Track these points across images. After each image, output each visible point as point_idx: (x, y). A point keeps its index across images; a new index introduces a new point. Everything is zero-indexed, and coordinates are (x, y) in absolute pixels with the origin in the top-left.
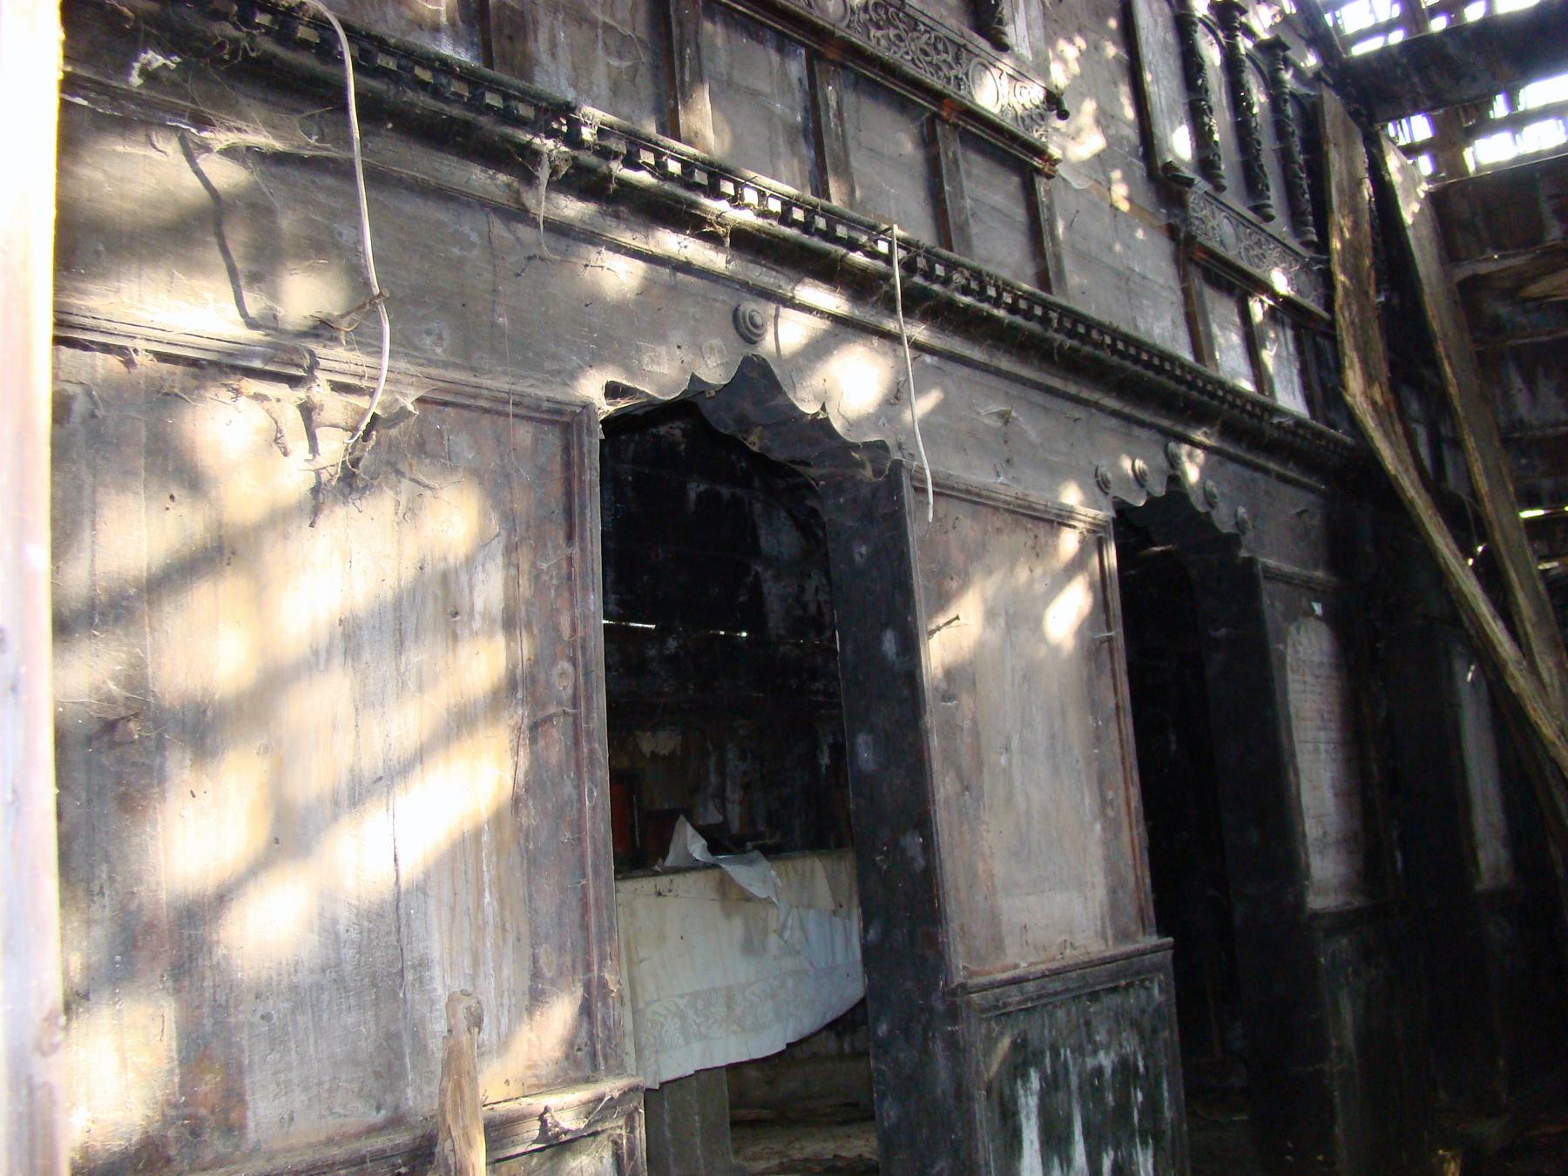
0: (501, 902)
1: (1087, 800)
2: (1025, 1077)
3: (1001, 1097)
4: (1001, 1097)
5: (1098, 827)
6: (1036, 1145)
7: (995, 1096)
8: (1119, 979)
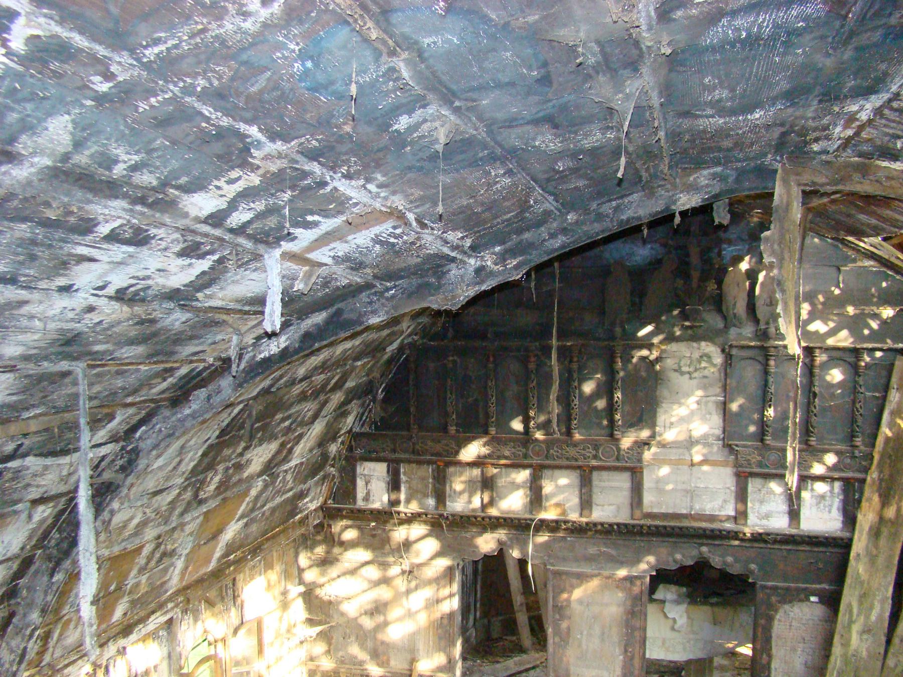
5: (621, 657)
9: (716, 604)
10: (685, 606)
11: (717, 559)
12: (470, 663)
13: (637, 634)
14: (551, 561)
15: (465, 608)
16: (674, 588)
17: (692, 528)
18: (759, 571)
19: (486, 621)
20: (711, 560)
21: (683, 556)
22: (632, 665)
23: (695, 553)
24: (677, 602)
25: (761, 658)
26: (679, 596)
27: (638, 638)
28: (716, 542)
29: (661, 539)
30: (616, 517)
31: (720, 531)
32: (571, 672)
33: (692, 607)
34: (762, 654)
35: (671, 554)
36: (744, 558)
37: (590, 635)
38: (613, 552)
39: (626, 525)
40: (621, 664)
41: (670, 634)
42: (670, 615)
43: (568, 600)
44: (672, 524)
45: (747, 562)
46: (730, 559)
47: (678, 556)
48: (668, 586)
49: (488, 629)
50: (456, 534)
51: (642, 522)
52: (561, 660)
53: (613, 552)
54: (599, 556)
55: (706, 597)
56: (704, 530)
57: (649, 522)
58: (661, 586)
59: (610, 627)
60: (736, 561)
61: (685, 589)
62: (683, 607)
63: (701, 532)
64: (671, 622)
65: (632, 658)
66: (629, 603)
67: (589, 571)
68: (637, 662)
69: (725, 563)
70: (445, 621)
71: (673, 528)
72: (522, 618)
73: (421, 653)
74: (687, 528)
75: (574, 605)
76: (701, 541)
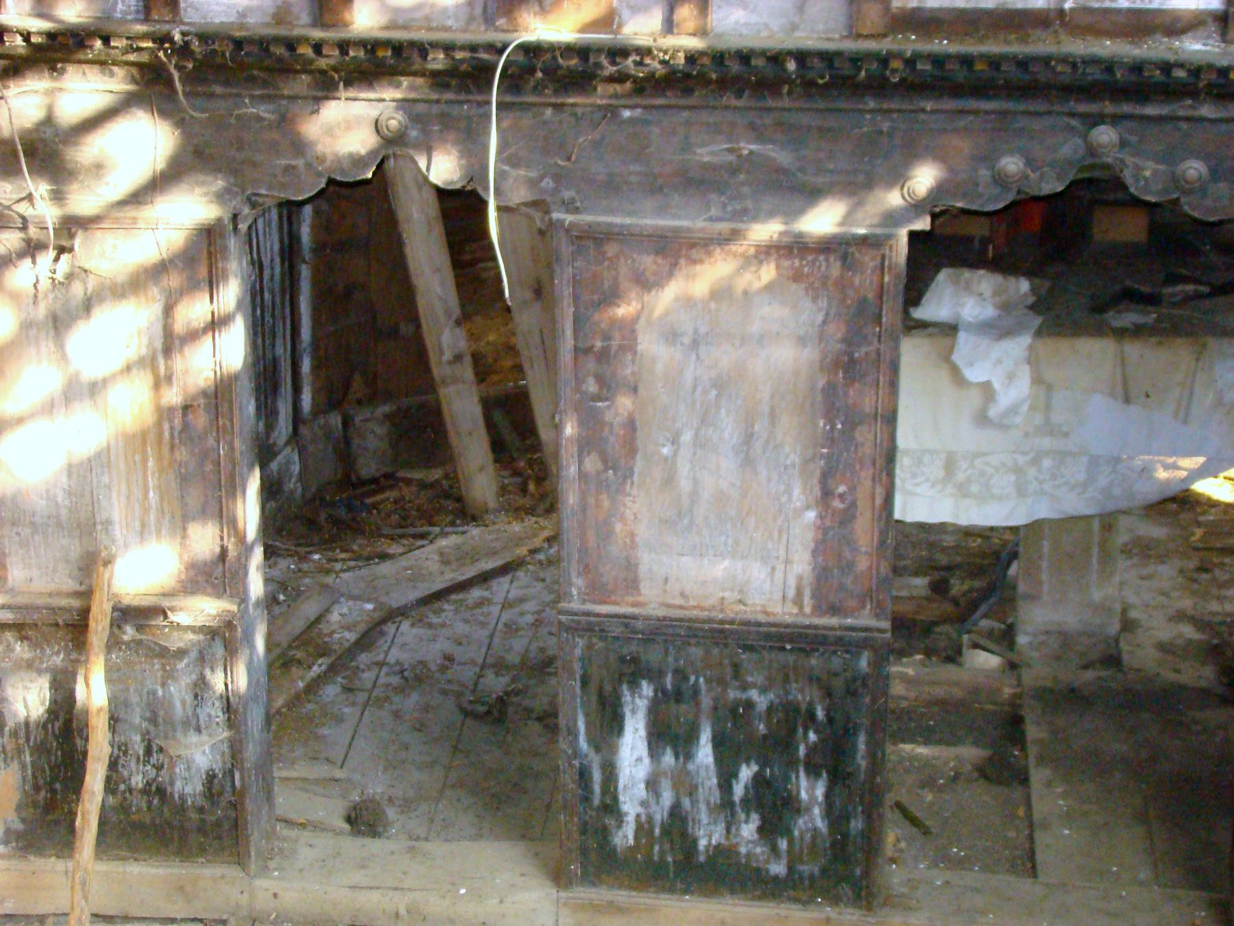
0: (162, 499)
1: (797, 492)
2: (634, 685)
3: (601, 689)
4: (601, 689)
5: (811, 515)
6: (642, 732)
7: (593, 687)
9: (1137, 332)
10: (1025, 340)
11: (1149, 169)
12: (286, 564)
13: (866, 436)
14: (567, 194)
15: (265, 373)
16: (986, 281)
17: (1064, 60)
19: (335, 420)
20: (1128, 176)
21: (1029, 162)
22: (850, 542)
23: (1070, 148)
24: (998, 330)
26: (1005, 308)
27: (867, 450)
28: (1151, 110)
29: (950, 104)
30: (794, 27)
31: (1166, 67)
32: (643, 570)
33: (1049, 346)
35: (988, 158)
37: (699, 443)
38: (783, 157)
39: (828, 58)
40: (810, 536)
41: (967, 438)
42: (975, 374)
43: (629, 328)
44: (993, 47)
46: (1194, 169)
47: (1012, 164)
48: (967, 274)
49: (344, 452)
50: (221, 106)
51: (884, 46)
52: (606, 533)
53: (783, 157)
54: (734, 171)
55: (1099, 308)
56: (1109, 66)
57: (912, 44)
58: (943, 276)
59: (773, 415)
60: (1216, 173)
61: (1024, 285)
63: (1095, 73)
64: (974, 399)
65: (847, 518)
66: (837, 331)
67: (700, 224)
68: (864, 531)
69: (1175, 180)
70: (201, 420)
71: (995, 62)
72: (462, 406)
73: (118, 531)
74: (1046, 60)
75: (648, 343)
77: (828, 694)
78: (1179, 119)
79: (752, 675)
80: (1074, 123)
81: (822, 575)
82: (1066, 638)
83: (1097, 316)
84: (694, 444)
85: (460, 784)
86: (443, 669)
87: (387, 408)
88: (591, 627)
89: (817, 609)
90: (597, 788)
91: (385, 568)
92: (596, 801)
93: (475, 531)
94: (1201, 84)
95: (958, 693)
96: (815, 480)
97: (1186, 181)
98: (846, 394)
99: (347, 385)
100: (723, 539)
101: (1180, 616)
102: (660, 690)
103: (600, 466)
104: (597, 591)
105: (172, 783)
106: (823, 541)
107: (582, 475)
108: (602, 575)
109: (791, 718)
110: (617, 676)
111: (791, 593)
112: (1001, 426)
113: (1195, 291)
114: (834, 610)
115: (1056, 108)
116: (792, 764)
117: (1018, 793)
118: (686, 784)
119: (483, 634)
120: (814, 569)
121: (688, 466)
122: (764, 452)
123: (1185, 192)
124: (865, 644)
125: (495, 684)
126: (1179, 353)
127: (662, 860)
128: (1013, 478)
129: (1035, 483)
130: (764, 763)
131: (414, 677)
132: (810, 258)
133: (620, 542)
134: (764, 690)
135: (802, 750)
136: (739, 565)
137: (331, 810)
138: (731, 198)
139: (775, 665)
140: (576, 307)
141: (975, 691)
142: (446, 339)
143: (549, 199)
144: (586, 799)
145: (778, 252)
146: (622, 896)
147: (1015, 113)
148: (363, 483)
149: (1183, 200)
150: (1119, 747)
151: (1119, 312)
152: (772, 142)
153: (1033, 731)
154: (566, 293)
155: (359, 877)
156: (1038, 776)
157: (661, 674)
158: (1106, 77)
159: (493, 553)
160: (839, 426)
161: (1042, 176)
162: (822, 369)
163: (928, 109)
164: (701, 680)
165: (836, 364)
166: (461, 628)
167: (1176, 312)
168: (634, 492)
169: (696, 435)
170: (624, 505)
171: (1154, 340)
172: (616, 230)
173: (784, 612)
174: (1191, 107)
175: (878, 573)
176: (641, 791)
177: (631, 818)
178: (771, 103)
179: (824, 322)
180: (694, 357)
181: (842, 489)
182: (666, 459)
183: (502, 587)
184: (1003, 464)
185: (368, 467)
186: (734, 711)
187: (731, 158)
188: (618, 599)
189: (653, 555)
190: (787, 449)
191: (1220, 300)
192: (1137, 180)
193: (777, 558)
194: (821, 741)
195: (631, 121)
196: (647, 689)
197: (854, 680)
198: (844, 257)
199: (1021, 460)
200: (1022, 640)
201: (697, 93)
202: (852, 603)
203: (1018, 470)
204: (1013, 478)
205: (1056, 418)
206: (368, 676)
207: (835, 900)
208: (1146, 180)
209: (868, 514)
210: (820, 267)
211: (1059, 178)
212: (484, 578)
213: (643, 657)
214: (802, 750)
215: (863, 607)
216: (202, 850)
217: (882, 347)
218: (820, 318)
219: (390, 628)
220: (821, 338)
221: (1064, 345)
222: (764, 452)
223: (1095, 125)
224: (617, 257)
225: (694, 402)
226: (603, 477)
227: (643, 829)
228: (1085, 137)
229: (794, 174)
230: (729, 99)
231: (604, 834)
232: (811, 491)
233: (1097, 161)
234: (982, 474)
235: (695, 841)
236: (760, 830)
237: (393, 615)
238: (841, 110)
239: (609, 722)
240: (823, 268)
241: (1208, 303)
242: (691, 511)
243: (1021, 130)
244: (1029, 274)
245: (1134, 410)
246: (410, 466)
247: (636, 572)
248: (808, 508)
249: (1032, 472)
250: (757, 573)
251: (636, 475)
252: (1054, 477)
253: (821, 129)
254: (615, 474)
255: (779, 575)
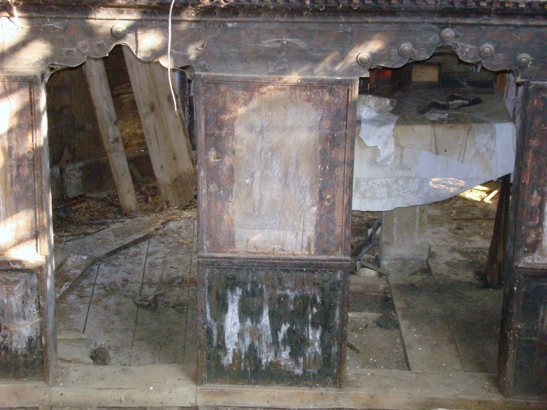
0: (6, 209)
1: (308, 199)
2: (233, 289)
3: (217, 293)
4: (217, 293)
5: (315, 209)
6: (237, 311)
7: (214, 290)
8: (303, 267)
9: (441, 122)
10: (392, 126)
11: (468, 48)
13: (339, 172)
18: (534, 63)
20: (458, 51)
21: (414, 46)
22: (332, 221)
23: (433, 39)
24: (378, 122)
25: (530, 198)
27: (341, 178)
28: (469, 21)
29: (378, 19)
32: (237, 237)
33: (402, 129)
34: (532, 193)
36: (510, 45)
37: (262, 177)
38: (302, 45)
40: (314, 218)
45: (516, 51)
46: (488, 47)
47: (406, 46)
52: (220, 220)
53: (302, 45)
54: (280, 51)
55: (422, 112)
59: (297, 163)
60: (498, 49)
61: (388, 101)
62: (388, 130)
65: (331, 210)
66: (327, 124)
67: (264, 76)
68: (339, 215)
69: (480, 54)
70: (26, 171)
72: (119, 163)
76: (443, 20)
77: (323, 290)
78: (481, 25)
79: (287, 283)
80: (435, 27)
81: (319, 236)
82: (404, 261)
83: (422, 116)
84: (261, 178)
85: (141, 339)
86: (124, 285)
87: (80, 164)
88: (214, 263)
89: (317, 252)
90: (215, 338)
91: (88, 239)
92: (215, 344)
93: (128, 221)
94: (493, 9)
95: (360, 288)
96: (316, 193)
97: (485, 53)
98: (331, 153)
99: (61, 154)
100: (274, 221)
101: (453, 250)
102: (245, 292)
103: (217, 189)
104: (215, 247)
105: (11, 344)
106: (320, 221)
107: (209, 193)
108: (218, 240)
109: (305, 302)
110: (225, 285)
111: (305, 245)
112: (382, 165)
113: (462, 103)
114: (325, 252)
115: (426, 20)
116: (306, 323)
117: (395, 332)
118: (256, 334)
119: (140, 268)
120: (316, 233)
121: (258, 188)
122: (293, 181)
123: (484, 58)
124: (340, 267)
125: (150, 292)
126: (460, 131)
127: (245, 370)
128: (386, 189)
129: (395, 191)
130: (293, 323)
131: (111, 290)
132: (314, 91)
133: (226, 224)
134: (293, 290)
135: (310, 317)
136: (282, 232)
137: (82, 354)
138: (279, 64)
139: (298, 278)
140: (206, 116)
141: (367, 287)
142: (110, 131)
143: (193, 65)
144: (210, 343)
145: (300, 89)
146: (226, 387)
147: (408, 23)
148: (70, 200)
149: (483, 62)
150: (436, 309)
151: (431, 113)
152: (297, 37)
153: (398, 304)
154: (201, 109)
155: (101, 384)
156: (404, 324)
157: (245, 284)
158: (450, 6)
159: (138, 231)
160: (328, 168)
161: (420, 51)
162: (319, 141)
163: (370, 21)
164: (264, 286)
165: (327, 139)
166: (128, 266)
167: (455, 112)
168: (233, 200)
169: (262, 173)
170: (228, 207)
171: (449, 125)
172: (225, 79)
173: (302, 254)
174: (487, 19)
175: (345, 234)
176: (236, 338)
177: (231, 351)
178: (297, 19)
179: (321, 120)
180: (261, 137)
181: (329, 197)
182: (248, 185)
183: (144, 246)
184: (382, 183)
185: (72, 192)
186: (279, 300)
187: (279, 45)
188: (225, 250)
189: (242, 229)
190: (304, 179)
191: (474, 107)
192: (462, 53)
193: (299, 229)
194: (320, 312)
195: (232, 28)
196: (239, 291)
197: (334, 283)
198: (331, 91)
199: (389, 181)
200: (385, 263)
201: (263, 15)
202: (333, 249)
203: (388, 186)
204: (386, 189)
205: (405, 162)
206: (89, 290)
207: (324, 385)
208: (467, 53)
209: (341, 208)
210: (319, 94)
211: (428, 53)
212: (136, 243)
213: (237, 277)
214: (310, 317)
215: (338, 250)
216: (26, 375)
217: (348, 131)
218: (319, 118)
219: (95, 267)
220: (320, 127)
221: (409, 128)
222: (293, 181)
223: (444, 28)
224: (225, 92)
225: (261, 158)
226: (218, 194)
227: (237, 355)
228: (440, 33)
229: (307, 52)
230: (278, 18)
231: (218, 358)
232: (315, 198)
233: (445, 44)
234: (372, 187)
235: (260, 361)
236: (290, 354)
237: (96, 261)
238: (328, 22)
239: (221, 307)
240: (320, 96)
241: (468, 108)
242: (259, 209)
243: (411, 30)
244: (388, 97)
245: (440, 157)
246: (91, 191)
247: (233, 238)
248: (313, 206)
249: (394, 186)
250: (290, 236)
251: (234, 193)
252: (404, 189)
253: (320, 32)
254: (224, 192)
255: (300, 237)
